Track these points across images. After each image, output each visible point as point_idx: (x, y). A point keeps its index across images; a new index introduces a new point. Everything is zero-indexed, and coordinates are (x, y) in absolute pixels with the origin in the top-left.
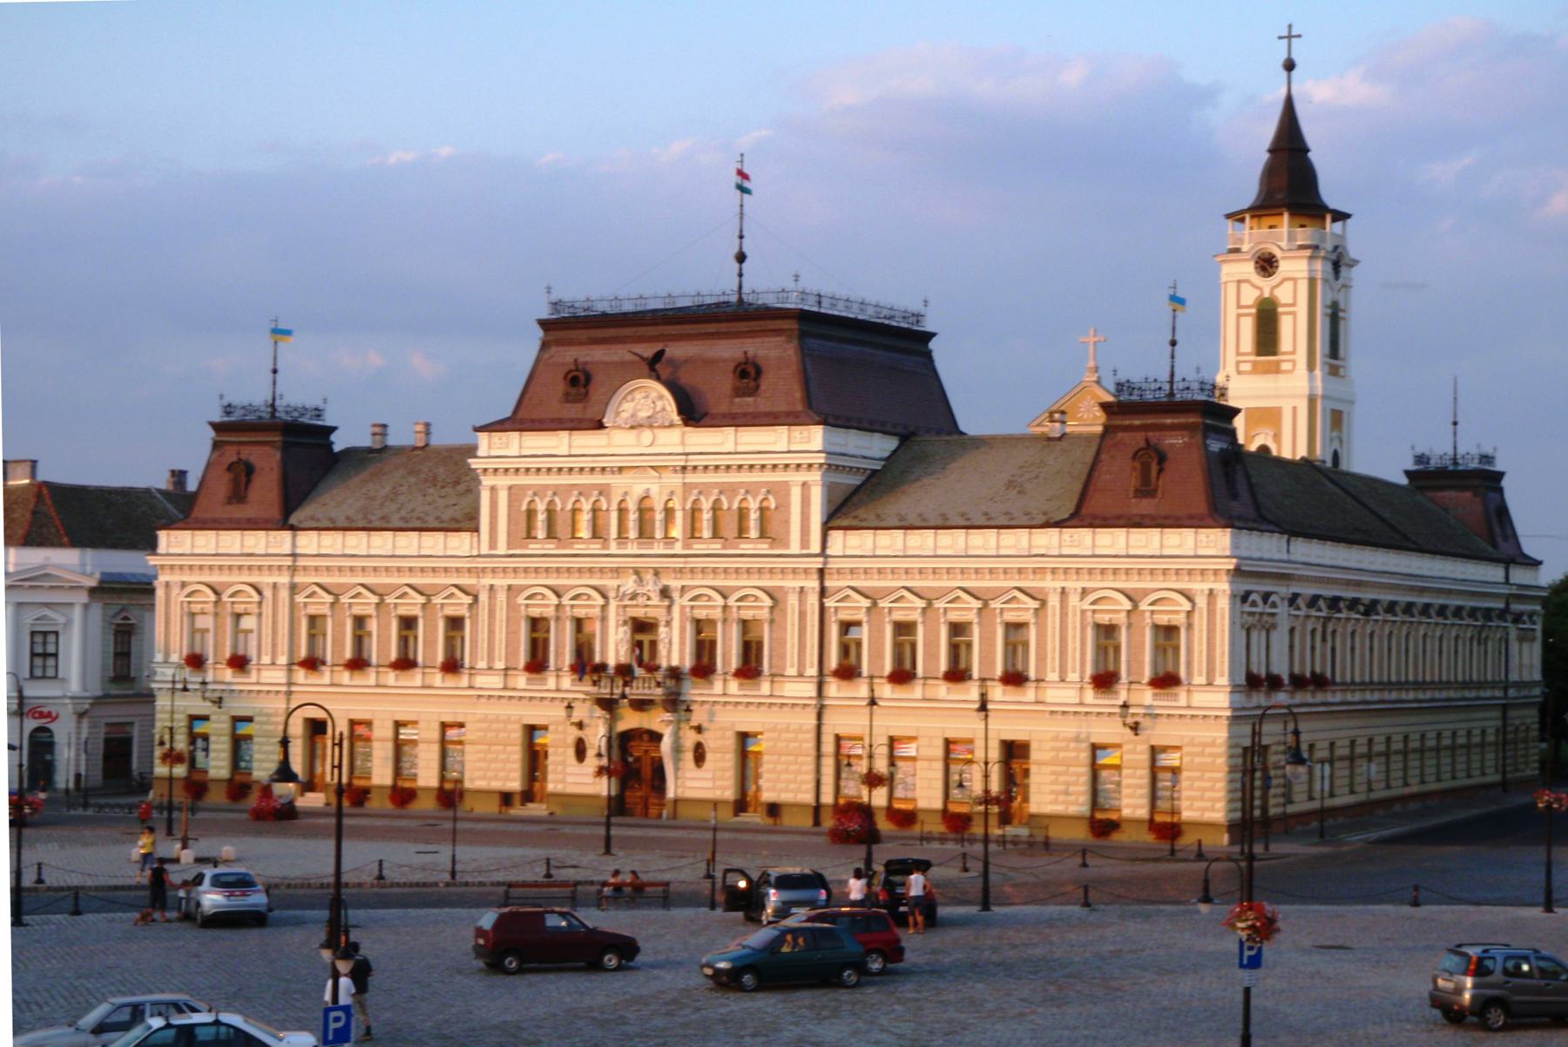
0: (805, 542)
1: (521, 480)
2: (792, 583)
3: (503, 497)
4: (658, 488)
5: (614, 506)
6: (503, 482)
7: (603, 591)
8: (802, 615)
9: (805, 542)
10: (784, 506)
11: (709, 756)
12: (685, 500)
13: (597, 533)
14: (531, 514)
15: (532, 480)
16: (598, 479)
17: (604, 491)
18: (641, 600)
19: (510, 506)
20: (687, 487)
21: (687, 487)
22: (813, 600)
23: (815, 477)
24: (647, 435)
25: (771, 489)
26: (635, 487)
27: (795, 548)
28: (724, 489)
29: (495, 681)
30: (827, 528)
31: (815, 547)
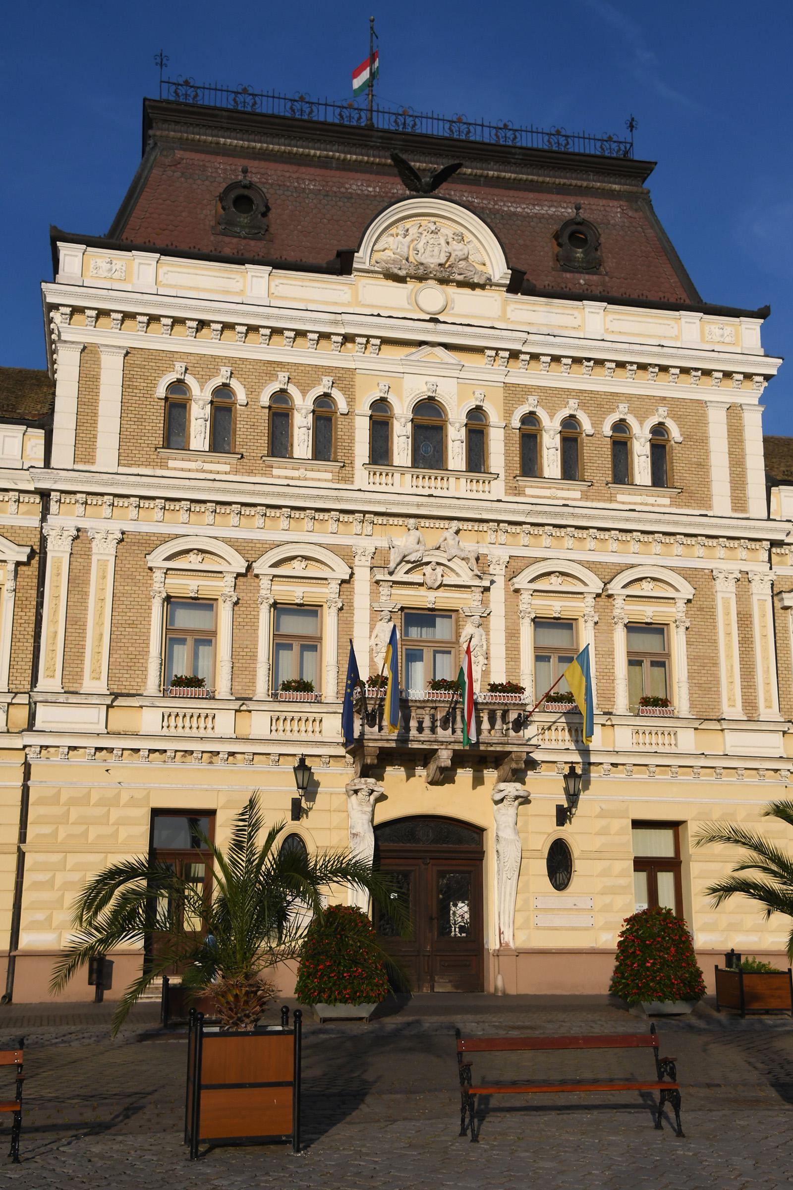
0: (739, 501)
1: (157, 340)
2: (725, 563)
3: (111, 371)
4: (458, 389)
5: (364, 408)
6: (112, 338)
7: (350, 552)
8: (745, 620)
9: (739, 501)
10: (698, 439)
11: (579, 866)
12: (508, 414)
13: (325, 446)
14: (176, 407)
15: (183, 342)
16: (329, 356)
17: (344, 379)
18: (430, 575)
19: (127, 385)
20: (514, 393)
21: (514, 393)
22: (761, 592)
23: (750, 396)
24: (432, 296)
25: (675, 405)
26: (408, 383)
27: (721, 502)
28: (588, 399)
29: (90, 718)
30: (772, 482)
31: (757, 507)
